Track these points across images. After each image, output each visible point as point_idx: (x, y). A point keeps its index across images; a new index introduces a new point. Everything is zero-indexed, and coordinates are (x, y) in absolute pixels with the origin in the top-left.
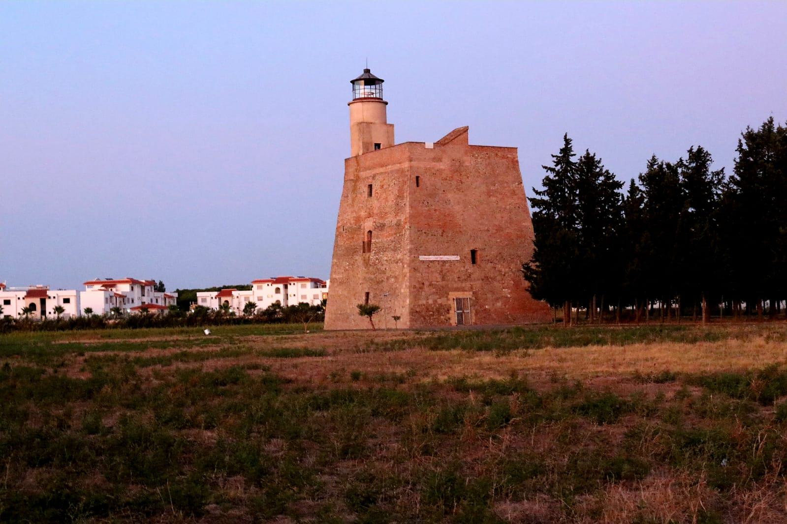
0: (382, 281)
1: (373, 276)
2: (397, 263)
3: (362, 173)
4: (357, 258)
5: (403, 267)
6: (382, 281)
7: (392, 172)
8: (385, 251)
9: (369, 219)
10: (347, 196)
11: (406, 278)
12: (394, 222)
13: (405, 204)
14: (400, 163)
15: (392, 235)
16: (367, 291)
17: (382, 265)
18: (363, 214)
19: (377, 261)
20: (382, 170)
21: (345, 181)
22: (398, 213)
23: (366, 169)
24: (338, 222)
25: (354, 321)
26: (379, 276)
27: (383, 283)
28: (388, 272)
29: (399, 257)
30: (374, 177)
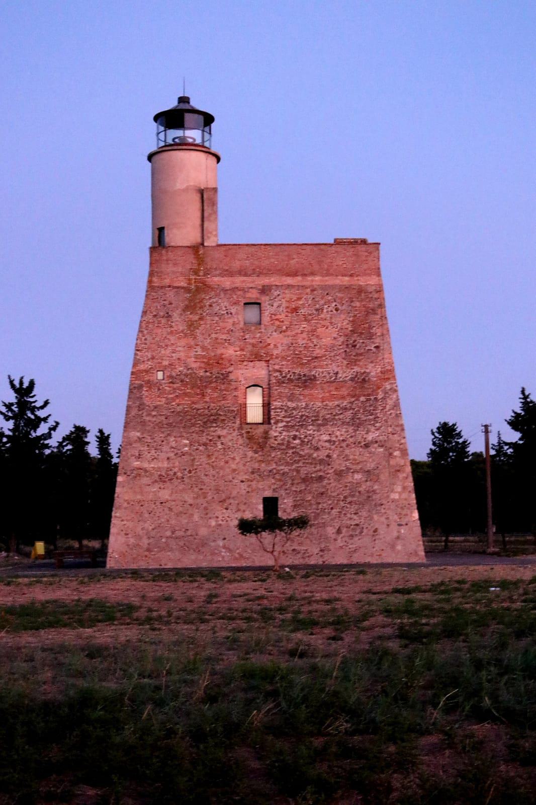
0: (321, 478)
1: (286, 469)
2: (367, 446)
3: (216, 279)
4: (220, 432)
5: (391, 454)
6: (321, 478)
7: (324, 288)
8: (323, 425)
9: (251, 364)
10: (168, 316)
11: (401, 476)
12: (346, 374)
13: (377, 347)
14: (351, 275)
15: (343, 398)
16: (268, 494)
17: (317, 449)
18: (230, 352)
19: (297, 441)
20: (289, 281)
21: (151, 287)
22: (356, 360)
23: (230, 273)
24: (136, 363)
25: (230, 550)
26: (311, 469)
27: (326, 481)
28: (338, 462)
29: (370, 437)
30: (265, 290)
